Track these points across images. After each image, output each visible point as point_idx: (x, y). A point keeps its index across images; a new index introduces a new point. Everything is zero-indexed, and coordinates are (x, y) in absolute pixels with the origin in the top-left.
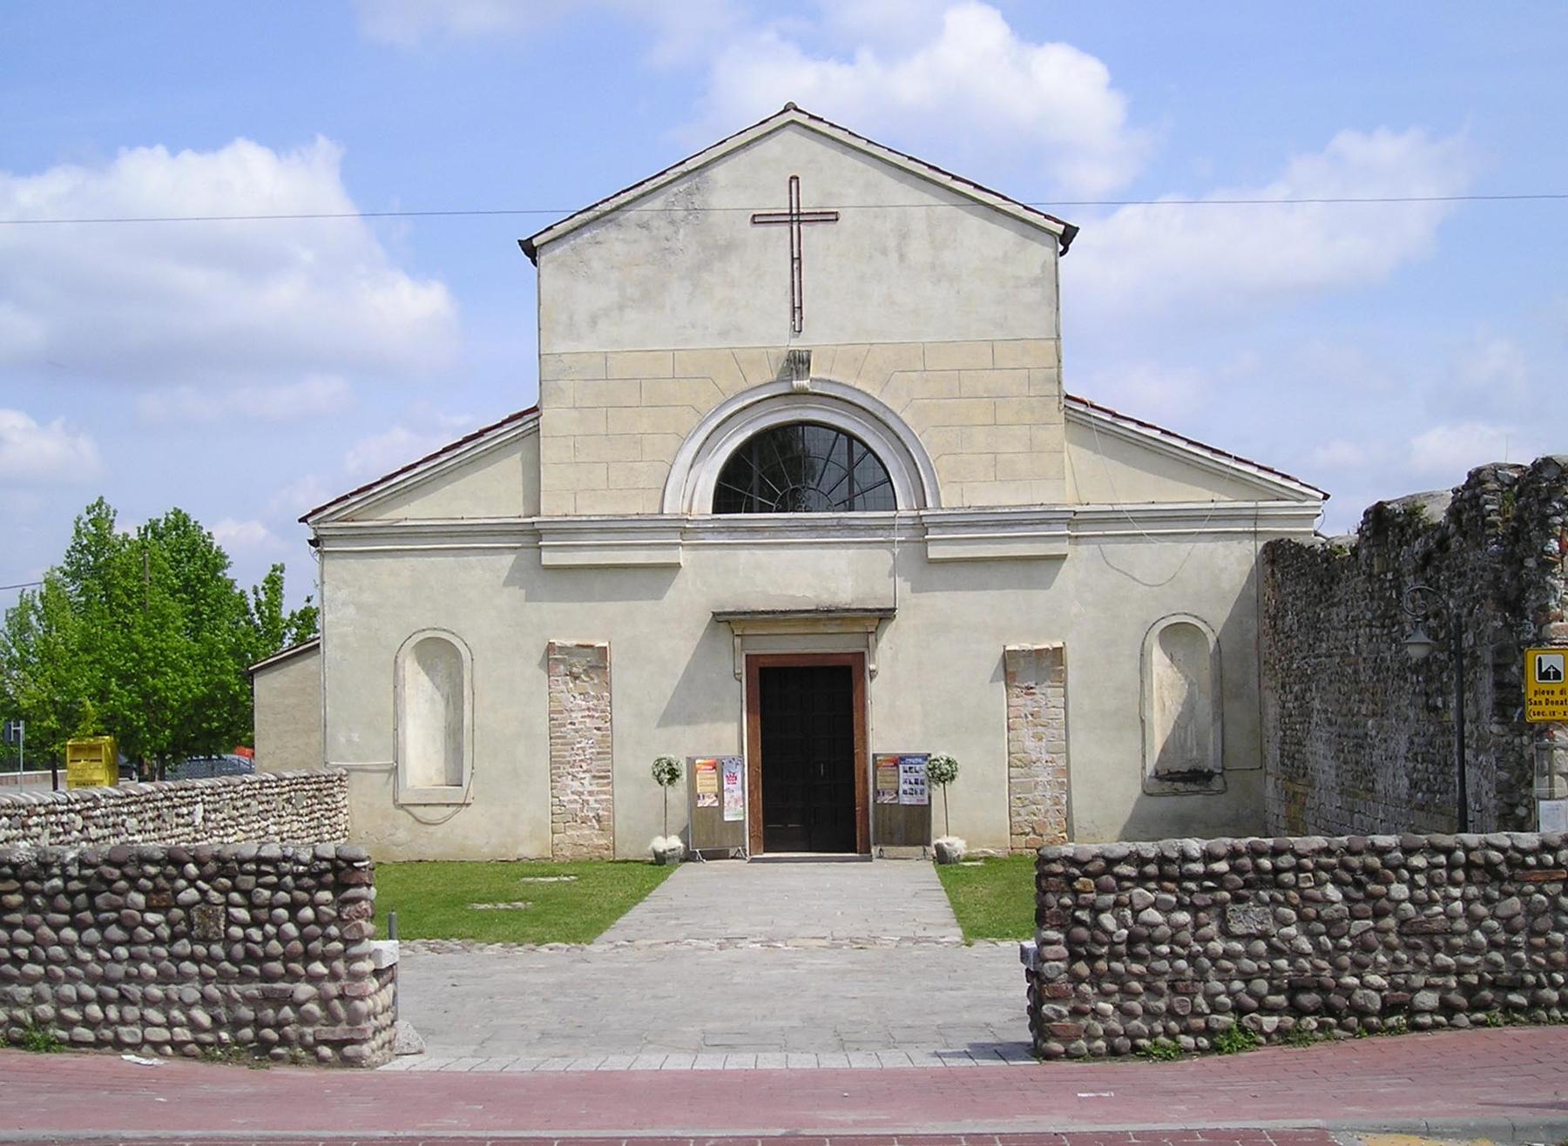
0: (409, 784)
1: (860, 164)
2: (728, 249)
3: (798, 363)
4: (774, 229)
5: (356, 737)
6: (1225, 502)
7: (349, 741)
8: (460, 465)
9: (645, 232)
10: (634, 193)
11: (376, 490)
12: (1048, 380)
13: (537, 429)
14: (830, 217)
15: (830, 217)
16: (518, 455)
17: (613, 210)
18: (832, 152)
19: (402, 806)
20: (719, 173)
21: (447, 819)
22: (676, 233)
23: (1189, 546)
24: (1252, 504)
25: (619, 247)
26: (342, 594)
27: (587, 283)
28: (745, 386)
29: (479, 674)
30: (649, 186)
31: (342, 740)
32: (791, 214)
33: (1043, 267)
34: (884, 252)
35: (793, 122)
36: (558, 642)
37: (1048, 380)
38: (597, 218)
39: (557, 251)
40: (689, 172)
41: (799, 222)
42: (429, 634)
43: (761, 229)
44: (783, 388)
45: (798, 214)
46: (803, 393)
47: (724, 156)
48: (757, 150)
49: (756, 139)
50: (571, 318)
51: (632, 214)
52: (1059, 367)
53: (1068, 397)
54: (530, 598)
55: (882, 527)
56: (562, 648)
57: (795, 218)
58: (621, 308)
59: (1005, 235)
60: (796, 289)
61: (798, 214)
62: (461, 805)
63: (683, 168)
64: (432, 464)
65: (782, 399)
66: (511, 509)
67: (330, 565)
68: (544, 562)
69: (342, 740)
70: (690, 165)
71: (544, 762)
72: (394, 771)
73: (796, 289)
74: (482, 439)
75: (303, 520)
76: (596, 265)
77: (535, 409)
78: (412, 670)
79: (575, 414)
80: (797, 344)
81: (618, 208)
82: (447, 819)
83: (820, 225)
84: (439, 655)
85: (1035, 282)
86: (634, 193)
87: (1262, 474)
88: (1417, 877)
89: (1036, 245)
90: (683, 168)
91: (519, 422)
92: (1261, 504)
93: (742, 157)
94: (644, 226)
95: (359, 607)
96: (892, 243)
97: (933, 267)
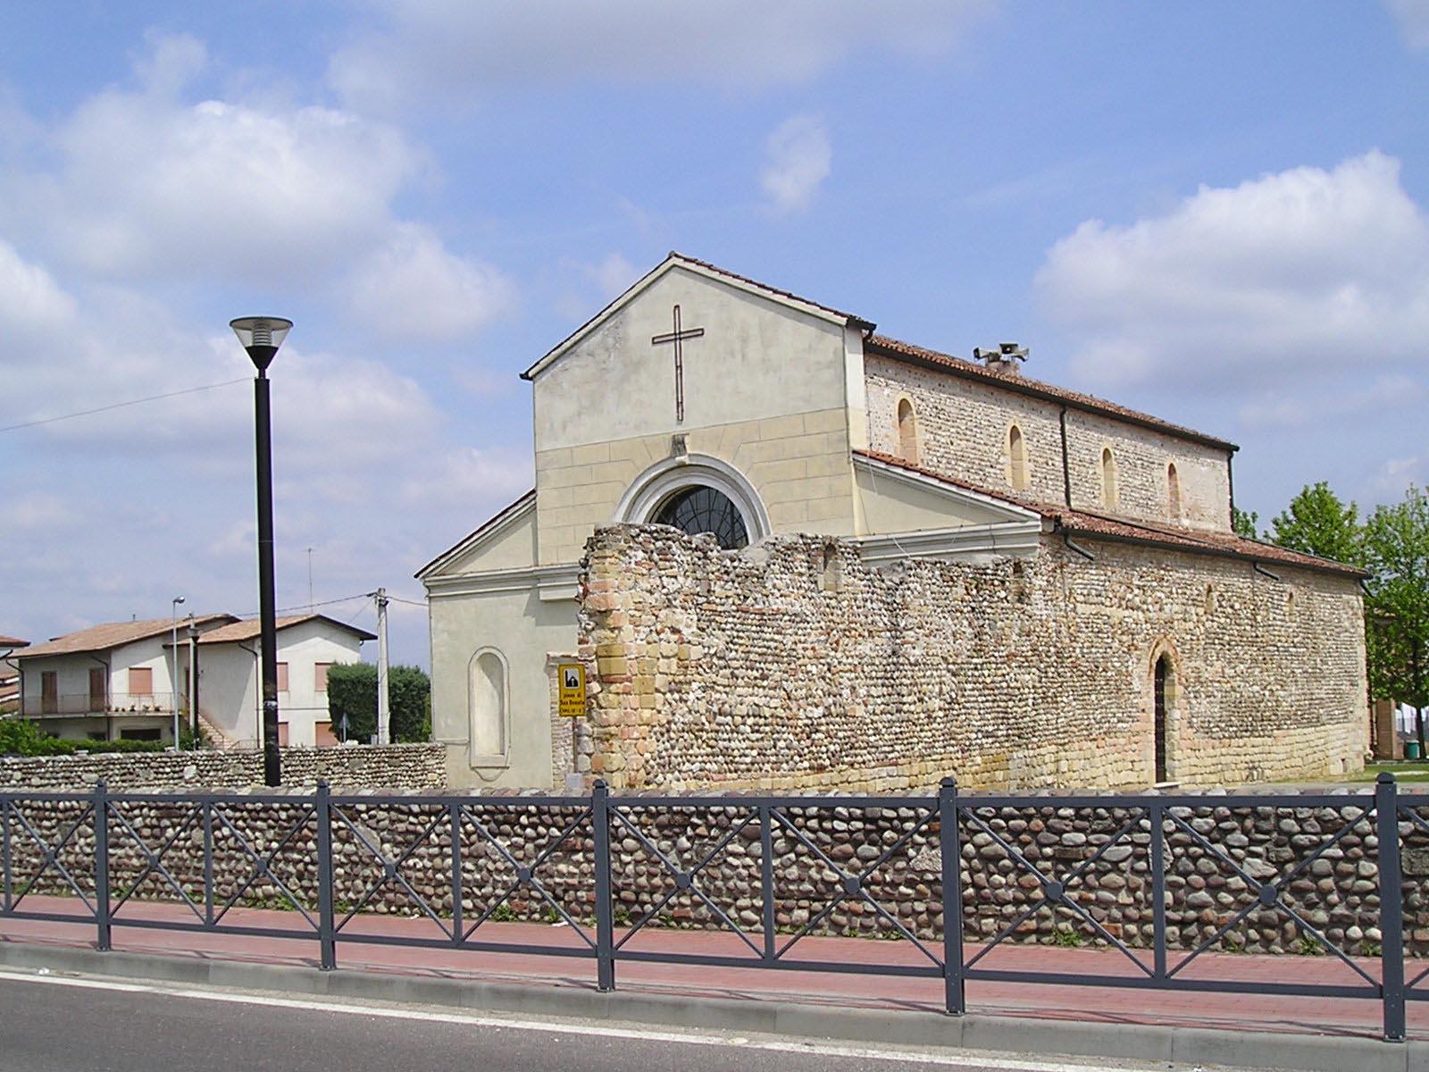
0: (477, 753)
1: (717, 291)
2: (639, 365)
3: (678, 444)
4: (666, 346)
5: (449, 721)
6: (970, 526)
7: (446, 723)
8: (498, 534)
9: (590, 358)
10: (583, 332)
11: (453, 553)
12: (840, 441)
13: (534, 507)
14: (700, 333)
15: (700, 333)
16: (530, 524)
17: (572, 346)
18: (699, 284)
19: (473, 769)
20: (633, 309)
21: (497, 777)
22: (609, 356)
23: (496, 599)
24: (987, 527)
25: (577, 371)
26: (440, 626)
27: (559, 400)
28: (652, 463)
29: (513, 675)
30: (591, 326)
31: (443, 725)
32: (675, 334)
33: (835, 352)
34: (732, 354)
35: (674, 266)
36: (552, 654)
37: (840, 441)
38: (565, 352)
39: (544, 379)
40: (615, 312)
41: (680, 339)
42: (486, 650)
43: (658, 347)
44: (671, 464)
45: (680, 333)
46: (682, 466)
47: (635, 296)
48: (655, 290)
49: (654, 281)
50: (552, 425)
51: (585, 345)
52: (848, 429)
53: (854, 452)
54: (537, 624)
55: (986, 538)
56: (554, 658)
57: (678, 337)
58: (579, 414)
59: (809, 331)
60: (679, 388)
61: (680, 333)
62: (502, 768)
63: (611, 310)
64: (481, 533)
65: (677, 470)
66: (524, 564)
67: (436, 605)
68: (541, 598)
69: (443, 725)
70: (615, 307)
71: (549, 739)
72: (469, 744)
73: (679, 388)
74: (507, 515)
75: (416, 576)
76: (565, 385)
77: (533, 492)
78: (478, 674)
79: (555, 493)
80: (679, 430)
81: (575, 343)
82: (497, 777)
83: (693, 340)
84: (491, 663)
85: (829, 365)
86: (583, 332)
87: (995, 502)
88: (1212, 835)
89: (831, 336)
90: (611, 310)
91: (526, 501)
92: (993, 527)
93: (646, 295)
94: (591, 354)
95: (450, 633)
96: (737, 346)
97: (764, 360)
